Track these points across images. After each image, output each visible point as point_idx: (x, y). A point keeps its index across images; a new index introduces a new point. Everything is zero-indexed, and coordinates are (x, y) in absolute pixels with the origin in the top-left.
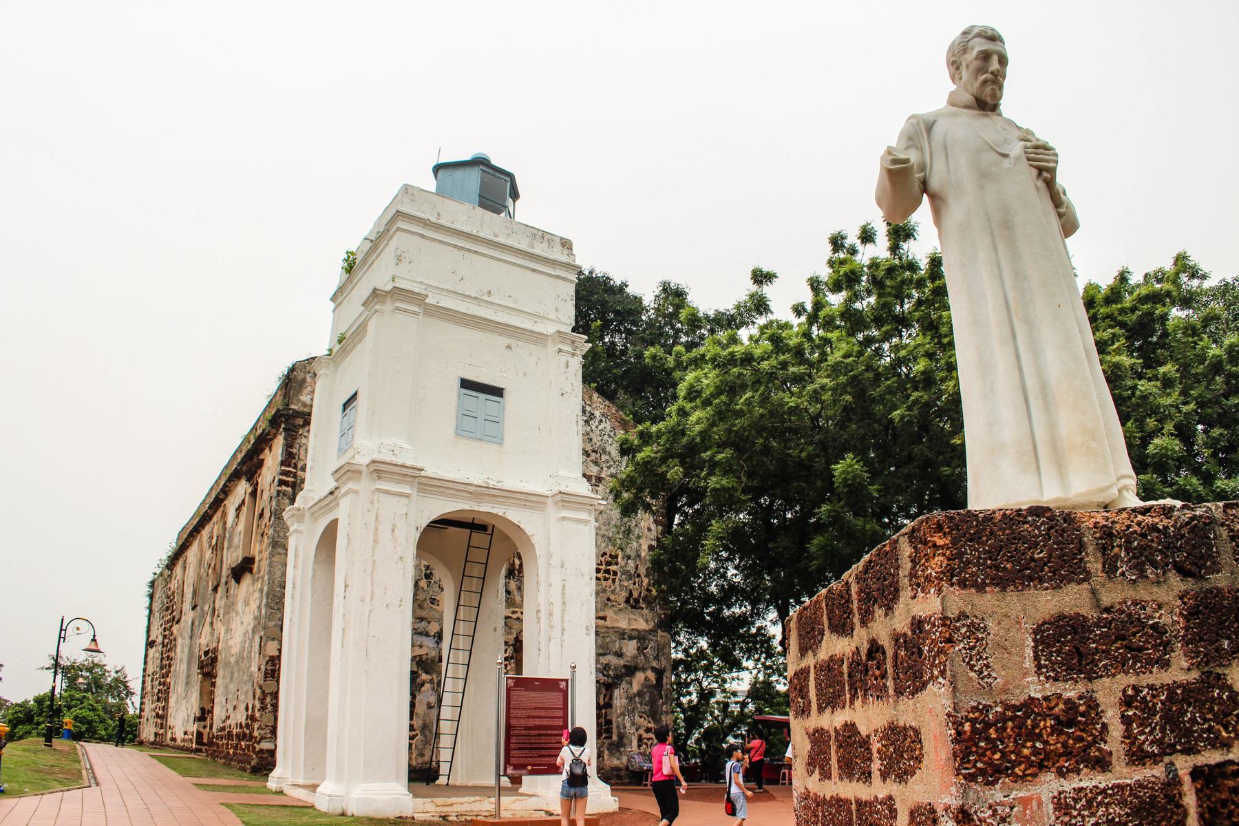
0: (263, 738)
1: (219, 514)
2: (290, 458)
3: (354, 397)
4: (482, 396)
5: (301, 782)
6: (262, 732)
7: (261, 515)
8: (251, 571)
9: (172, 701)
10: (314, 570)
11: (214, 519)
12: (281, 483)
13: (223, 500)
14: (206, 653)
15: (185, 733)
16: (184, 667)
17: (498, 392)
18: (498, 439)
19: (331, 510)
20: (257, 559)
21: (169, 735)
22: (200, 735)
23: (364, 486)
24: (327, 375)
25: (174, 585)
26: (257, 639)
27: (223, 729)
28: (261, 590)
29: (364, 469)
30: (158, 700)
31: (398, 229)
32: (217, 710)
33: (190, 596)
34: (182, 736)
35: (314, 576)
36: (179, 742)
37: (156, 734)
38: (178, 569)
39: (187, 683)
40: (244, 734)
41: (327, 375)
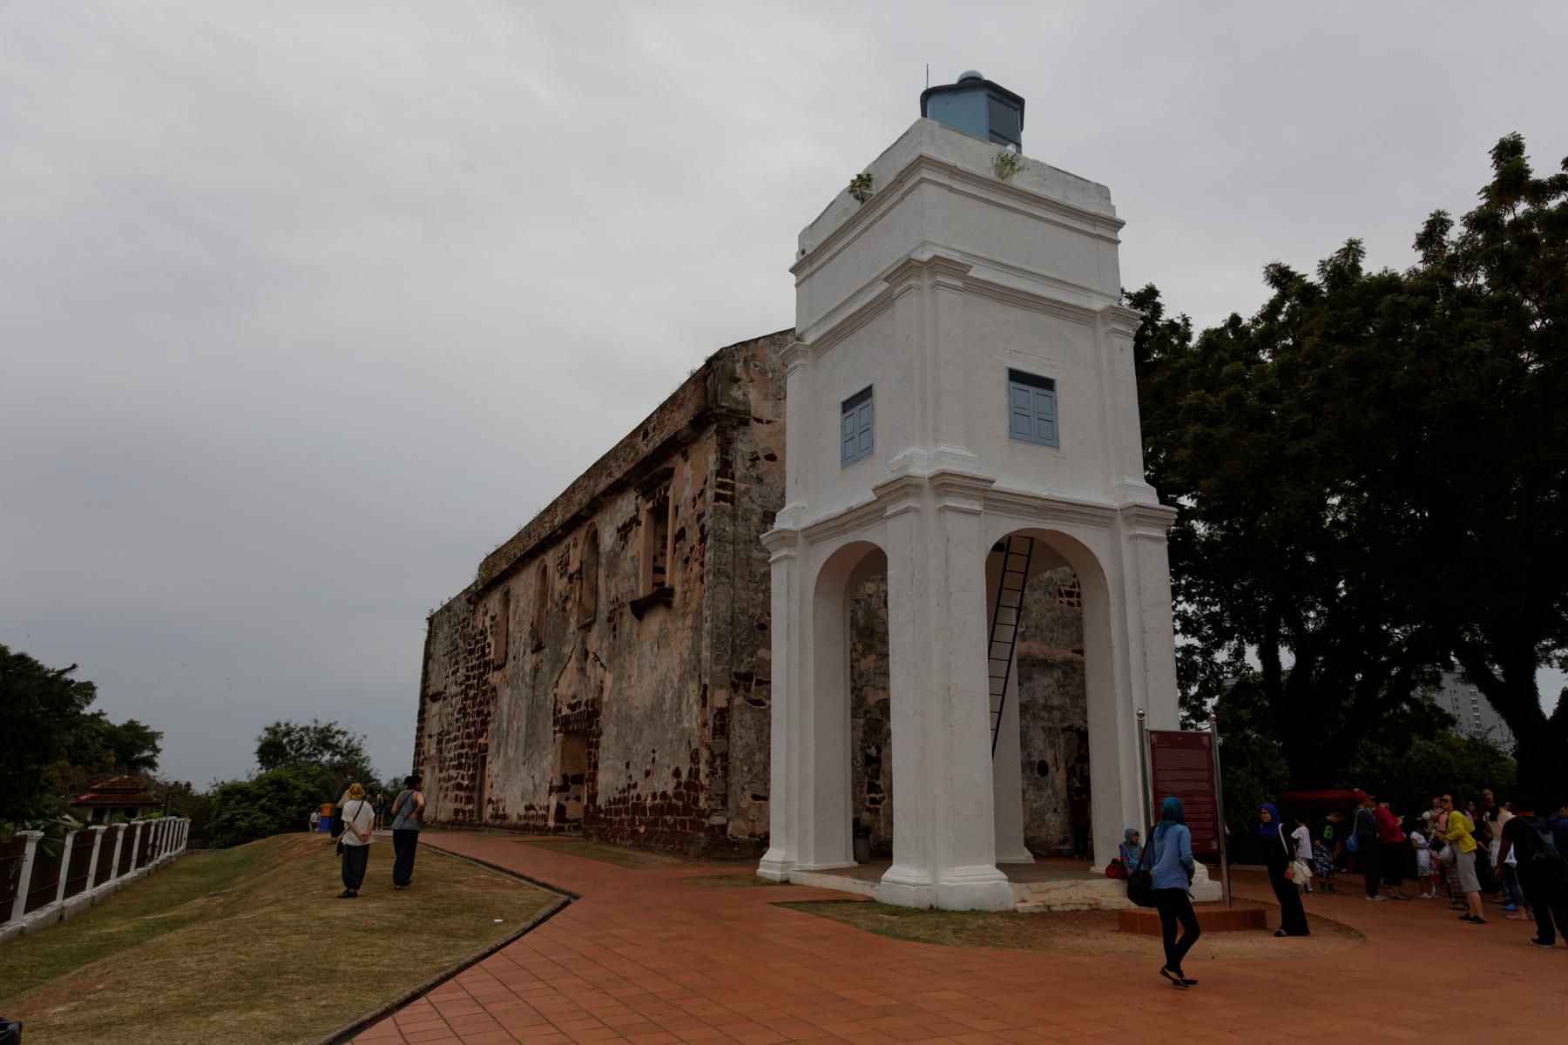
0: (713, 811)
1: (581, 534)
2: (725, 468)
3: (867, 393)
4: (1032, 390)
5: (811, 865)
6: (712, 804)
7: (681, 535)
8: (669, 605)
9: (494, 767)
10: (815, 602)
11: (570, 540)
12: (718, 497)
13: (586, 519)
14: (572, 707)
15: (529, 808)
16: (520, 724)
17: (1047, 384)
18: (1052, 441)
19: (846, 532)
20: (678, 589)
21: (489, 811)
22: (561, 809)
23: (929, 503)
24: (804, 366)
25: (482, 621)
26: (693, 688)
27: (625, 800)
28: (697, 629)
29: (927, 483)
30: (460, 766)
31: (922, 180)
32: (604, 778)
33: (525, 636)
34: (522, 812)
35: (815, 611)
36: (514, 819)
37: (456, 811)
38: (494, 603)
39: (528, 745)
40: (672, 809)
41: (804, 366)
